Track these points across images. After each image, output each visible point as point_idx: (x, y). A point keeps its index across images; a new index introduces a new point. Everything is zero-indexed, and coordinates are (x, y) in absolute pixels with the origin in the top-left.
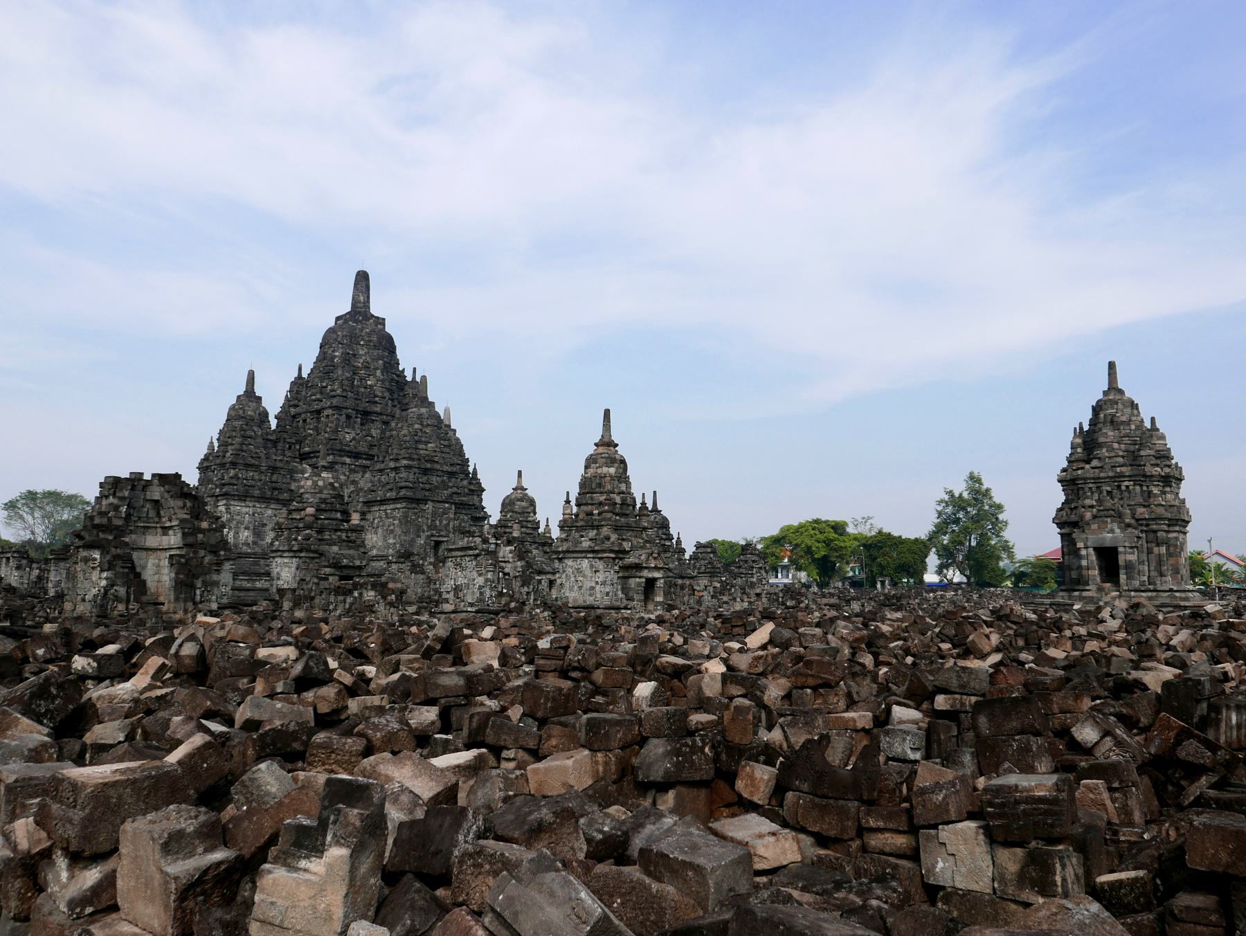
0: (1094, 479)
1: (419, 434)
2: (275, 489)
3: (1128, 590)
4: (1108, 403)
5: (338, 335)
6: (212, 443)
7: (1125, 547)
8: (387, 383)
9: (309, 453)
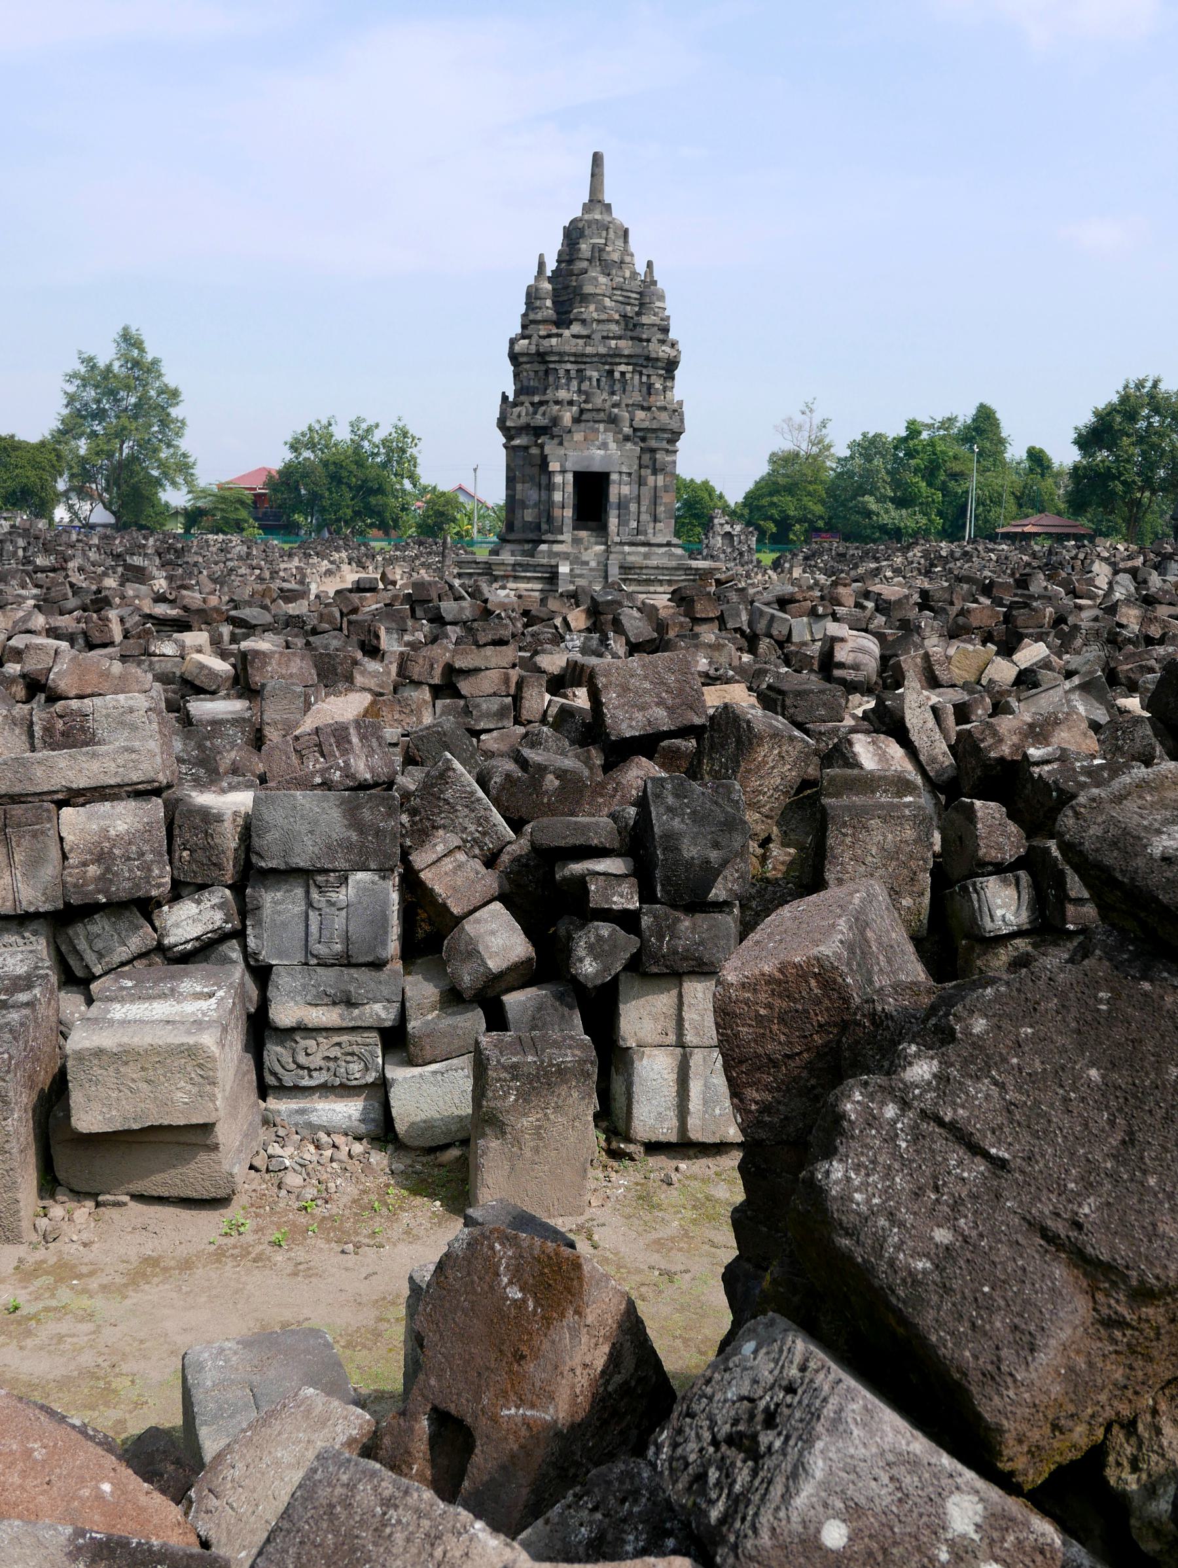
0: (575, 355)
3: (621, 544)
4: (594, 227)
7: (620, 473)
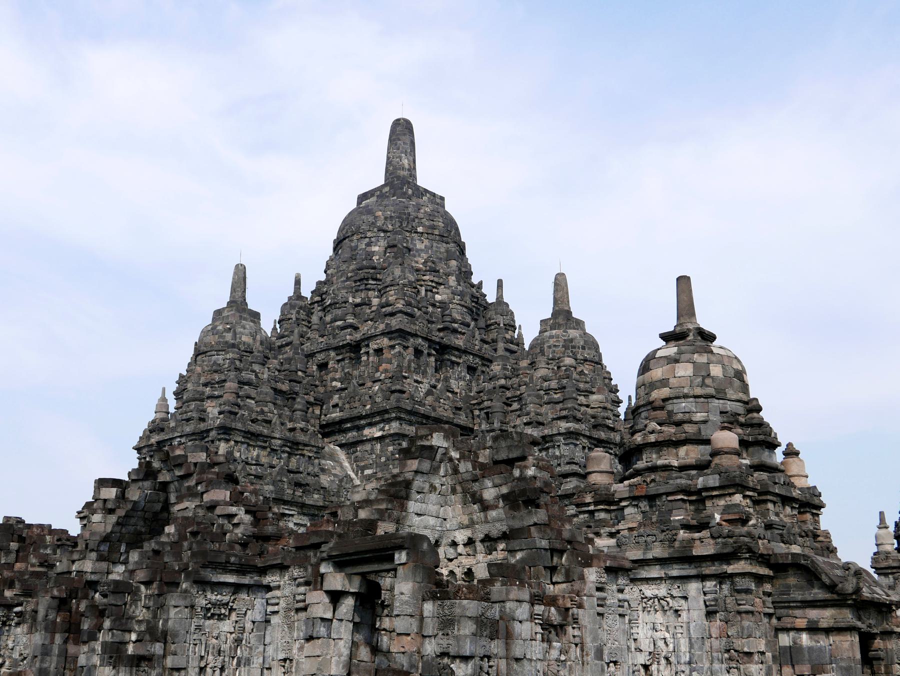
1: (575, 376)
2: (298, 485)
5: (376, 217)
6: (164, 399)
8: (468, 299)
9: (342, 421)
